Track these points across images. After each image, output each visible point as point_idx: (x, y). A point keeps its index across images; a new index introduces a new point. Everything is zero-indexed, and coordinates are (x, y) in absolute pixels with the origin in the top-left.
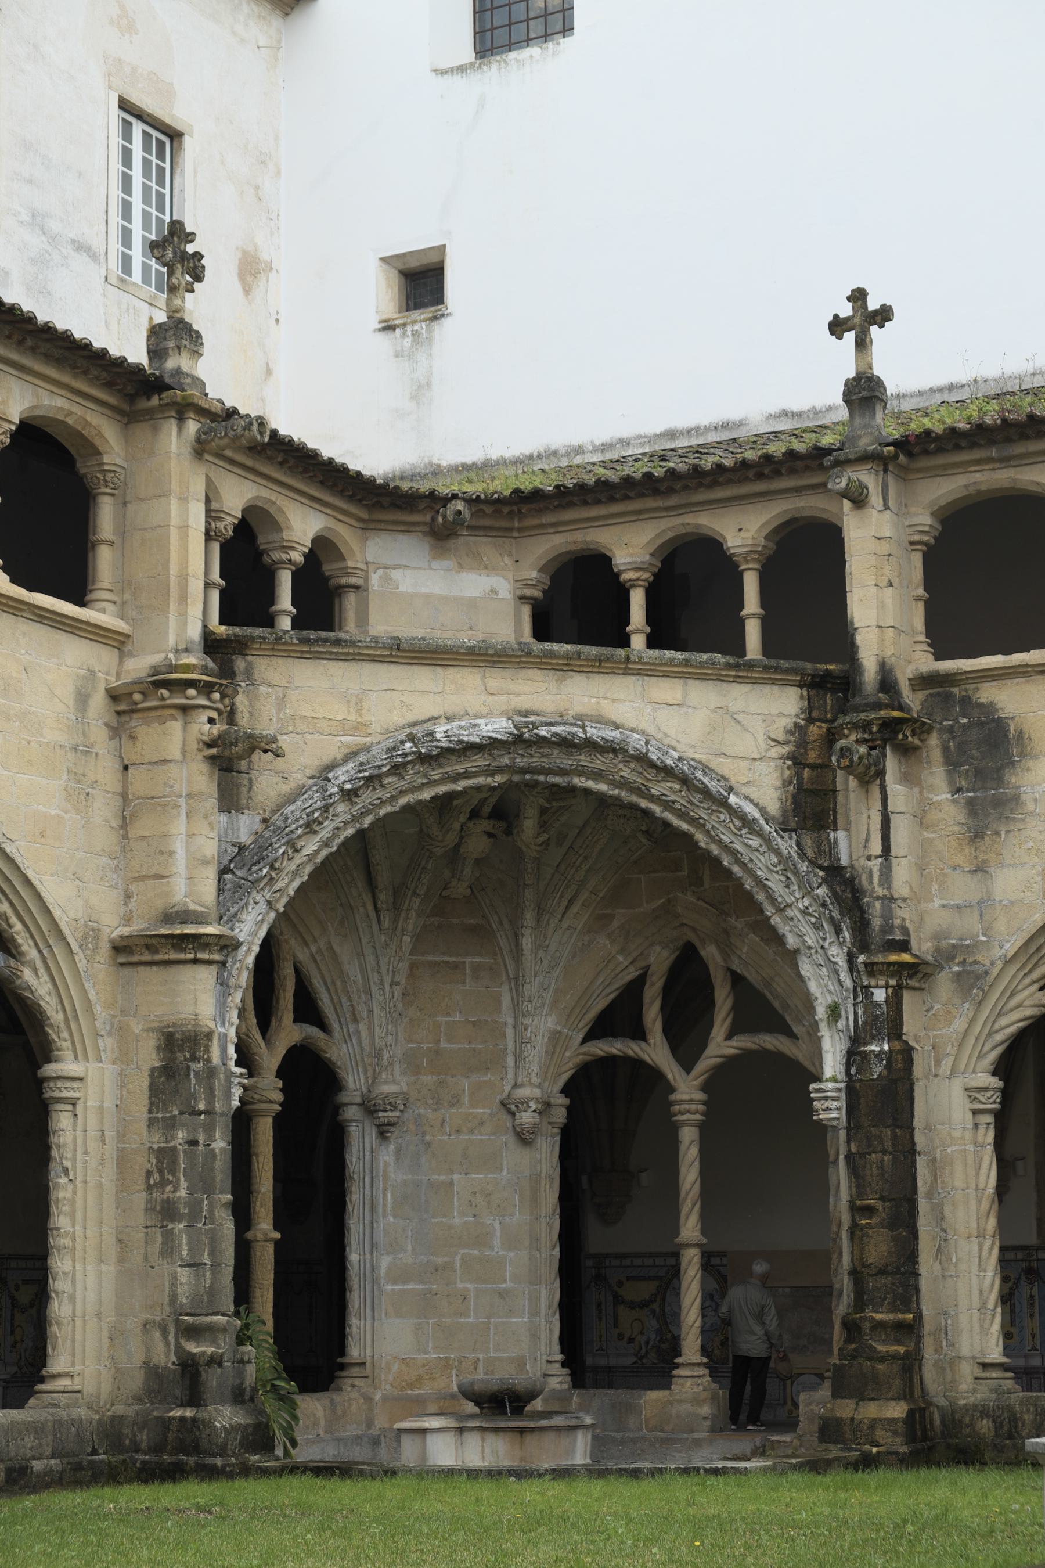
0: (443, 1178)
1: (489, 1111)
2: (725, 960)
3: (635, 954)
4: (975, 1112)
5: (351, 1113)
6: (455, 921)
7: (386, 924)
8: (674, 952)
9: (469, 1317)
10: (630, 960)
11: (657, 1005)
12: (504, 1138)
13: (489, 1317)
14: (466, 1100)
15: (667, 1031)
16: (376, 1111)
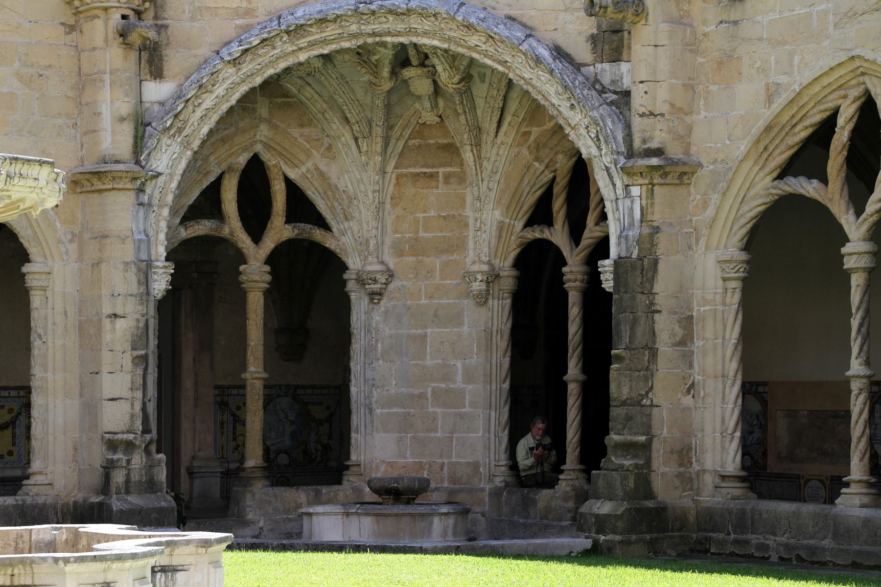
0: (419, 331)
4: (724, 280)
5: (351, 286)
7: (364, 149)
8: (571, 158)
9: (437, 432)
13: (452, 433)
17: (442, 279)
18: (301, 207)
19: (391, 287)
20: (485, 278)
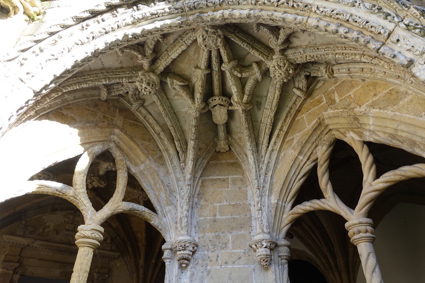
1: (243, 251)
2: (361, 137)
5: (166, 254)
6: (224, 161)
10: (306, 158)
11: (326, 176)
12: (252, 266)
14: (230, 245)
15: (337, 190)
16: (176, 251)
17: (234, 249)
18: (135, 191)
19: (197, 255)
20: (269, 244)
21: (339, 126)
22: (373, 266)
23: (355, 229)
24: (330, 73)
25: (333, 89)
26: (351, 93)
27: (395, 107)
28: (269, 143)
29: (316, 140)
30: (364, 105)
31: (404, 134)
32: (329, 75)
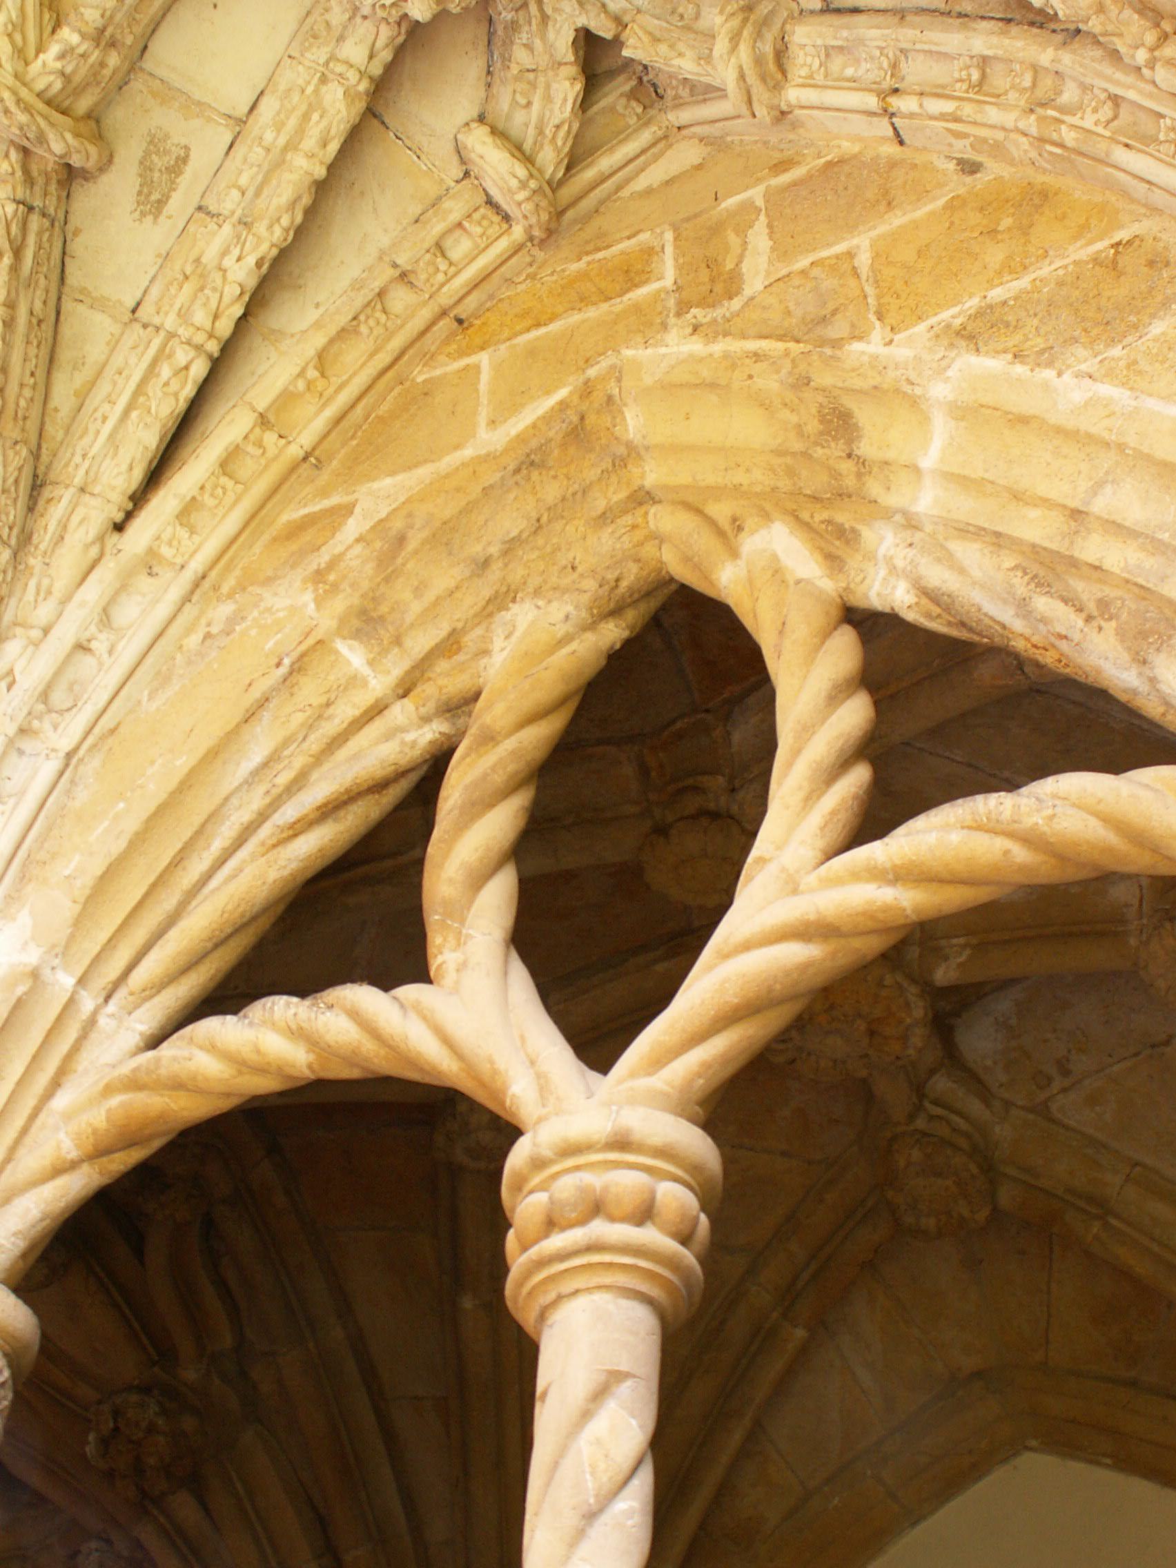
2: (833, 561)
3: (420, 642)
11: (500, 823)
15: (532, 938)
21: (708, 473)
22: (609, 1472)
23: (567, 1186)
24: (759, 61)
25: (748, 208)
26: (862, 244)
27: (1116, 351)
28: (139, 499)
29: (511, 547)
30: (921, 328)
31: (1116, 556)
32: (752, 79)
